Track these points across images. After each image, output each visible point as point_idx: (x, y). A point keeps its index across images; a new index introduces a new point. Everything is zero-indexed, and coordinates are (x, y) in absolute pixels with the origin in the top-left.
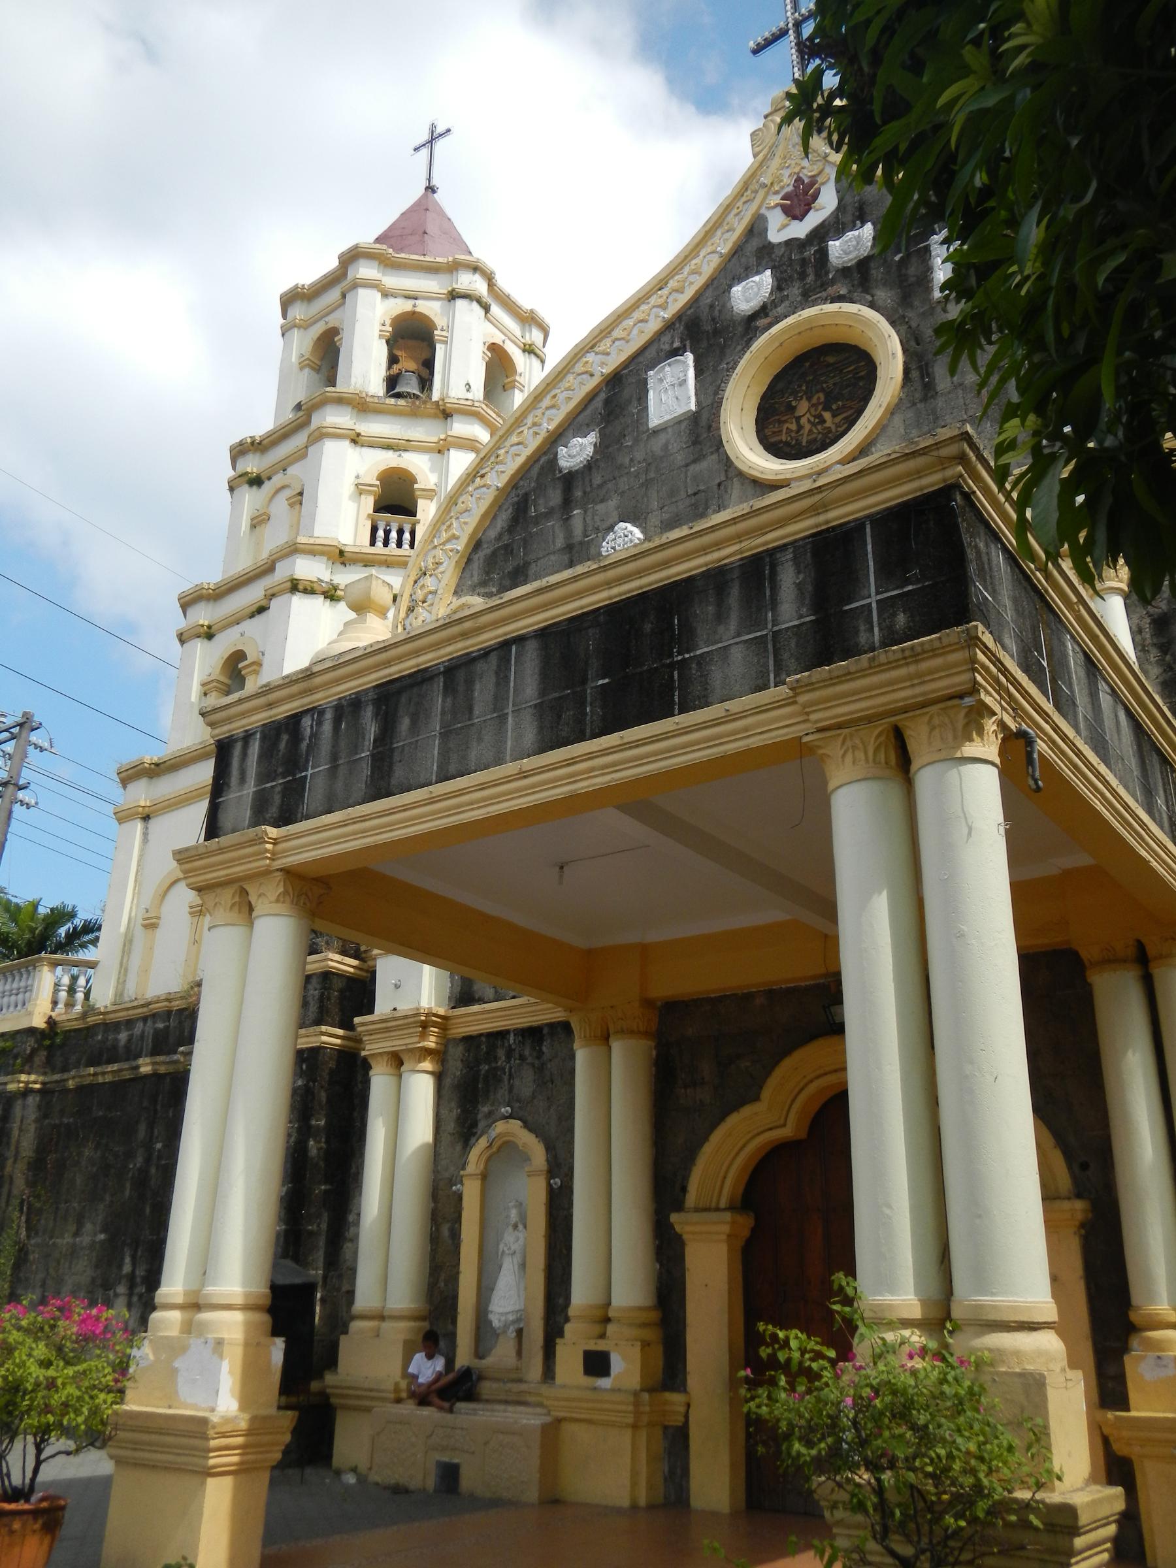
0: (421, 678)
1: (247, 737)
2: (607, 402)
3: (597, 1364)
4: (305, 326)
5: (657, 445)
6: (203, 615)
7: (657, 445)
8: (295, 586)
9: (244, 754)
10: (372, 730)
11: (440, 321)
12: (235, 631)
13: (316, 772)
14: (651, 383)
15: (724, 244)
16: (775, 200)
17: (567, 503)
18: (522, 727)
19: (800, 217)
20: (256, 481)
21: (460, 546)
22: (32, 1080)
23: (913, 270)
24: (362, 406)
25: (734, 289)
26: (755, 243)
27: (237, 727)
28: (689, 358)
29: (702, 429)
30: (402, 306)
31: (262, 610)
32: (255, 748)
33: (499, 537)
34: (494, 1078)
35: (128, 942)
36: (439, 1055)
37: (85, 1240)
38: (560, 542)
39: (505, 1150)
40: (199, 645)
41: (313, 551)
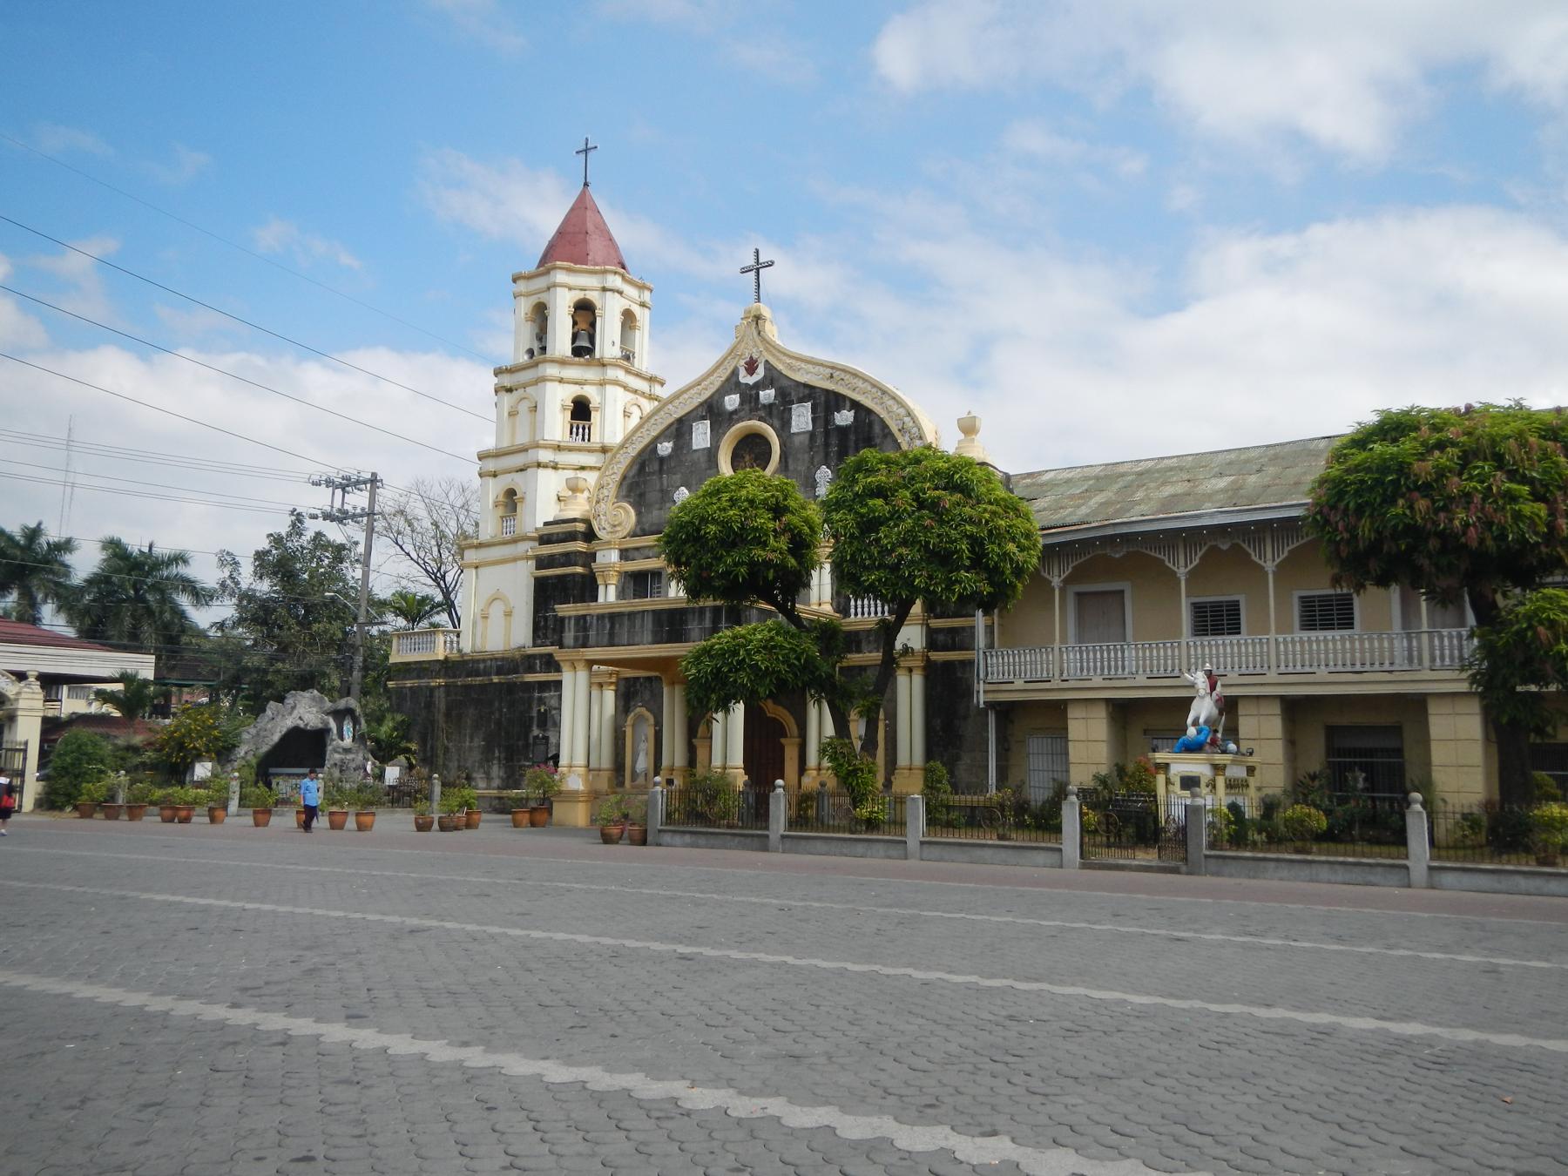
0: (621, 615)
4: (528, 295)
5: (695, 456)
6: (491, 465)
7: (695, 456)
8: (539, 465)
11: (598, 304)
12: (508, 477)
13: (592, 633)
15: (724, 374)
17: (661, 471)
18: (648, 636)
20: (510, 390)
21: (618, 478)
22: (441, 681)
24: (563, 363)
30: (579, 295)
34: (636, 693)
35: (475, 623)
36: (616, 684)
37: (475, 744)
39: (640, 718)
40: (491, 481)
41: (545, 447)
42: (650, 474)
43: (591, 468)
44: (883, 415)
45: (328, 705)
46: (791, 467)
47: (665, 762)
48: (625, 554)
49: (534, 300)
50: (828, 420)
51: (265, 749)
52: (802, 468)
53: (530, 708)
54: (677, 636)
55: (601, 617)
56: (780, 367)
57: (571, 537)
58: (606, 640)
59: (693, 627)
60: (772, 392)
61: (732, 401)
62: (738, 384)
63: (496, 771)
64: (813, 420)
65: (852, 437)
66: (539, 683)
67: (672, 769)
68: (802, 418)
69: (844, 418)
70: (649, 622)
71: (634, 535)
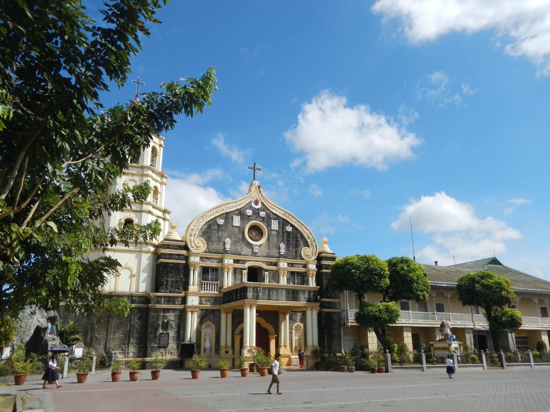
0: (273, 289)
1: (250, 287)
3: (227, 352)
8: (150, 212)
13: (260, 294)
17: (218, 230)
23: (269, 223)
26: (250, 205)
27: (249, 286)
29: (241, 230)
31: (136, 211)
32: (251, 289)
38: (217, 236)
42: (213, 230)
43: (161, 218)
44: (302, 231)
45: (45, 314)
46: (271, 240)
47: (223, 343)
48: (202, 258)
50: (283, 229)
51: (28, 339)
52: (275, 242)
53: (158, 319)
54: (295, 299)
55: (264, 289)
56: (267, 206)
58: (266, 298)
59: (301, 296)
61: (249, 212)
62: (251, 207)
63: (132, 349)
65: (291, 235)
67: (226, 347)
68: (275, 225)
69: (289, 229)
70: (284, 292)
71: (205, 252)
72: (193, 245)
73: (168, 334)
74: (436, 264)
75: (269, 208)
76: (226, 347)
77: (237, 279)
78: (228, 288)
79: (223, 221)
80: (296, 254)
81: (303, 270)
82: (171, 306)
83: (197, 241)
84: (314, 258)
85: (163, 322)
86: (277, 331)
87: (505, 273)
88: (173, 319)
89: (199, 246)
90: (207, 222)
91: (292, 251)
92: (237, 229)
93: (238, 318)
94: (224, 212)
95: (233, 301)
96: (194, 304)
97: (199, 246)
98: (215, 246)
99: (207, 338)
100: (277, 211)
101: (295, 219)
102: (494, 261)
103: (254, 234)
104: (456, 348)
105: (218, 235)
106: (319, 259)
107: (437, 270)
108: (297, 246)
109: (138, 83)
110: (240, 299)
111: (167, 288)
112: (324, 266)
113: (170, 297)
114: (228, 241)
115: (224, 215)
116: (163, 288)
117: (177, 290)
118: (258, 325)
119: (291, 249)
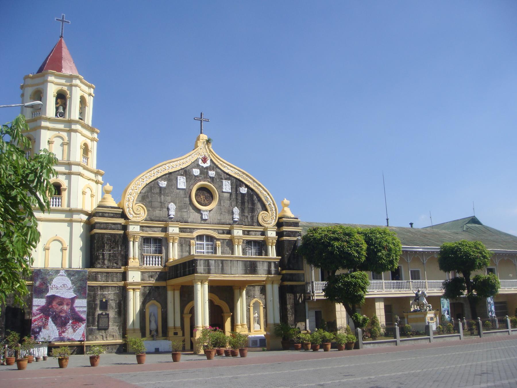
2: (169, 177)
3: (176, 334)
8: (79, 174)
9: (200, 263)
10: (221, 265)
13: (212, 268)
14: (178, 179)
16: (201, 157)
19: (204, 163)
25: (194, 170)
26: (196, 163)
28: (185, 178)
29: (187, 192)
30: (82, 93)
32: (202, 262)
33: (145, 193)
38: (159, 200)
42: (154, 193)
44: (258, 192)
46: (222, 204)
47: (171, 324)
49: (60, 87)
50: (236, 191)
57: (115, 216)
60: (214, 172)
61: (196, 172)
64: (231, 188)
65: (246, 198)
66: (101, 286)
67: (175, 328)
68: (227, 186)
69: (243, 190)
71: (146, 220)
72: (132, 212)
73: (108, 314)
74: (411, 227)
75: (219, 166)
76: (175, 328)
77: (184, 250)
78: (175, 261)
79: (166, 183)
80: (253, 219)
81: (260, 238)
82: (110, 283)
83: (136, 207)
84: (274, 223)
85: (101, 301)
86: (233, 309)
87: (485, 233)
88: (113, 298)
89: (137, 213)
90: (147, 185)
91: (247, 217)
92: (182, 192)
93: (188, 295)
94: (166, 172)
95: (181, 276)
96: (135, 281)
97: (137, 213)
98: (157, 213)
99: (153, 319)
100: (228, 169)
101: (251, 178)
102: (474, 220)
103: (202, 197)
104: (432, 319)
105: (161, 199)
106: (279, 224)
107: (412, 233)
108: (253, 210)
109: (63, 21)
110: (189, 274)
111: (103, 263)
112: (285, 233)
113: (108, 273)
114: (172, 206)
115: (167, 176)
116: (99, 263)
117: (115, 265)
118: (211, 302)
119: (246, 214)
